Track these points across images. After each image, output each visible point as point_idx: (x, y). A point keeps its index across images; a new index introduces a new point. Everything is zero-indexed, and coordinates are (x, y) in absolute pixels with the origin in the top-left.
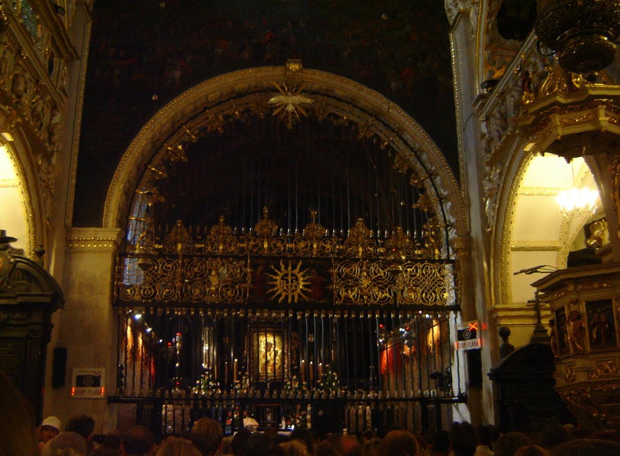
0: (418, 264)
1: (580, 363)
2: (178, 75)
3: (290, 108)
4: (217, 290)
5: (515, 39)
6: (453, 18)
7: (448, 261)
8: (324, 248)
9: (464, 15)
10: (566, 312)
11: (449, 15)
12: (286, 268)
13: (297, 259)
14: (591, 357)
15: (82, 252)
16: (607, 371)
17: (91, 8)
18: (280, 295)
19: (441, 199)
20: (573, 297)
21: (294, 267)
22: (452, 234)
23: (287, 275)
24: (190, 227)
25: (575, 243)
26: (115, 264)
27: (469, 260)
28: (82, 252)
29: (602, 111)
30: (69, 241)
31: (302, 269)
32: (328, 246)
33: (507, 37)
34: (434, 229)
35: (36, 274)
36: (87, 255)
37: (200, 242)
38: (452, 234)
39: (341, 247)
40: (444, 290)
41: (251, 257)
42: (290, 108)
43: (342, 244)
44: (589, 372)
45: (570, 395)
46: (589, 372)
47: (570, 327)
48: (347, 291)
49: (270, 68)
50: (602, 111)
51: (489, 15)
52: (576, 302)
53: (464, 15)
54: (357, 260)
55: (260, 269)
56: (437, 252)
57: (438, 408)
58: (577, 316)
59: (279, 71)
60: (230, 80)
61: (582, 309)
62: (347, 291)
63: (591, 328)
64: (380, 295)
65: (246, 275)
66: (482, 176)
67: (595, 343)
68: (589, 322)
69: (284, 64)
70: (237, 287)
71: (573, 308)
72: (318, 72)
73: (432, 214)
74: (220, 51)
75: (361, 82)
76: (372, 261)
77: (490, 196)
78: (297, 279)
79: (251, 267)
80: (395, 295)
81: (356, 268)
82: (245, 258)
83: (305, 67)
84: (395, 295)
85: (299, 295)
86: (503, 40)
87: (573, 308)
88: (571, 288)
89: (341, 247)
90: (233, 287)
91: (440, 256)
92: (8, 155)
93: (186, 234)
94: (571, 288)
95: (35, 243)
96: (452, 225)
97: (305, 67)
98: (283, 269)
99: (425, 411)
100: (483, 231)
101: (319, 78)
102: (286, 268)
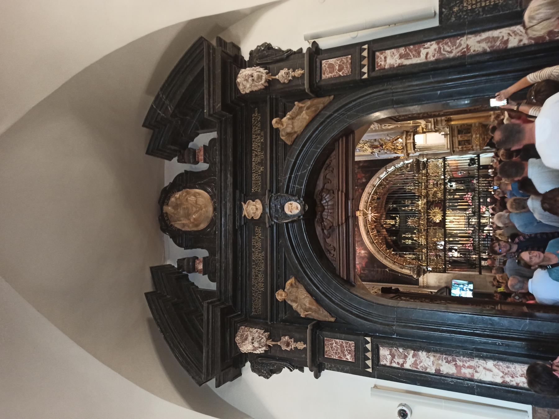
2: (363, 252)
15: (427, 282)
21: (430, 213)
28: (427, 282)
29: (408, 141)
30: (424, 287)
36: (429, 281)
42: (373, 214)
46: (476, 146)
52: (458, 148)
57: (482, 166)
58: (462, 148)
61: (460, 147)
63: (465, 145)
76: (427, 187)
81: (430, 192)
83: (358, 210)
97: (358, 210)
101: (362, 206)
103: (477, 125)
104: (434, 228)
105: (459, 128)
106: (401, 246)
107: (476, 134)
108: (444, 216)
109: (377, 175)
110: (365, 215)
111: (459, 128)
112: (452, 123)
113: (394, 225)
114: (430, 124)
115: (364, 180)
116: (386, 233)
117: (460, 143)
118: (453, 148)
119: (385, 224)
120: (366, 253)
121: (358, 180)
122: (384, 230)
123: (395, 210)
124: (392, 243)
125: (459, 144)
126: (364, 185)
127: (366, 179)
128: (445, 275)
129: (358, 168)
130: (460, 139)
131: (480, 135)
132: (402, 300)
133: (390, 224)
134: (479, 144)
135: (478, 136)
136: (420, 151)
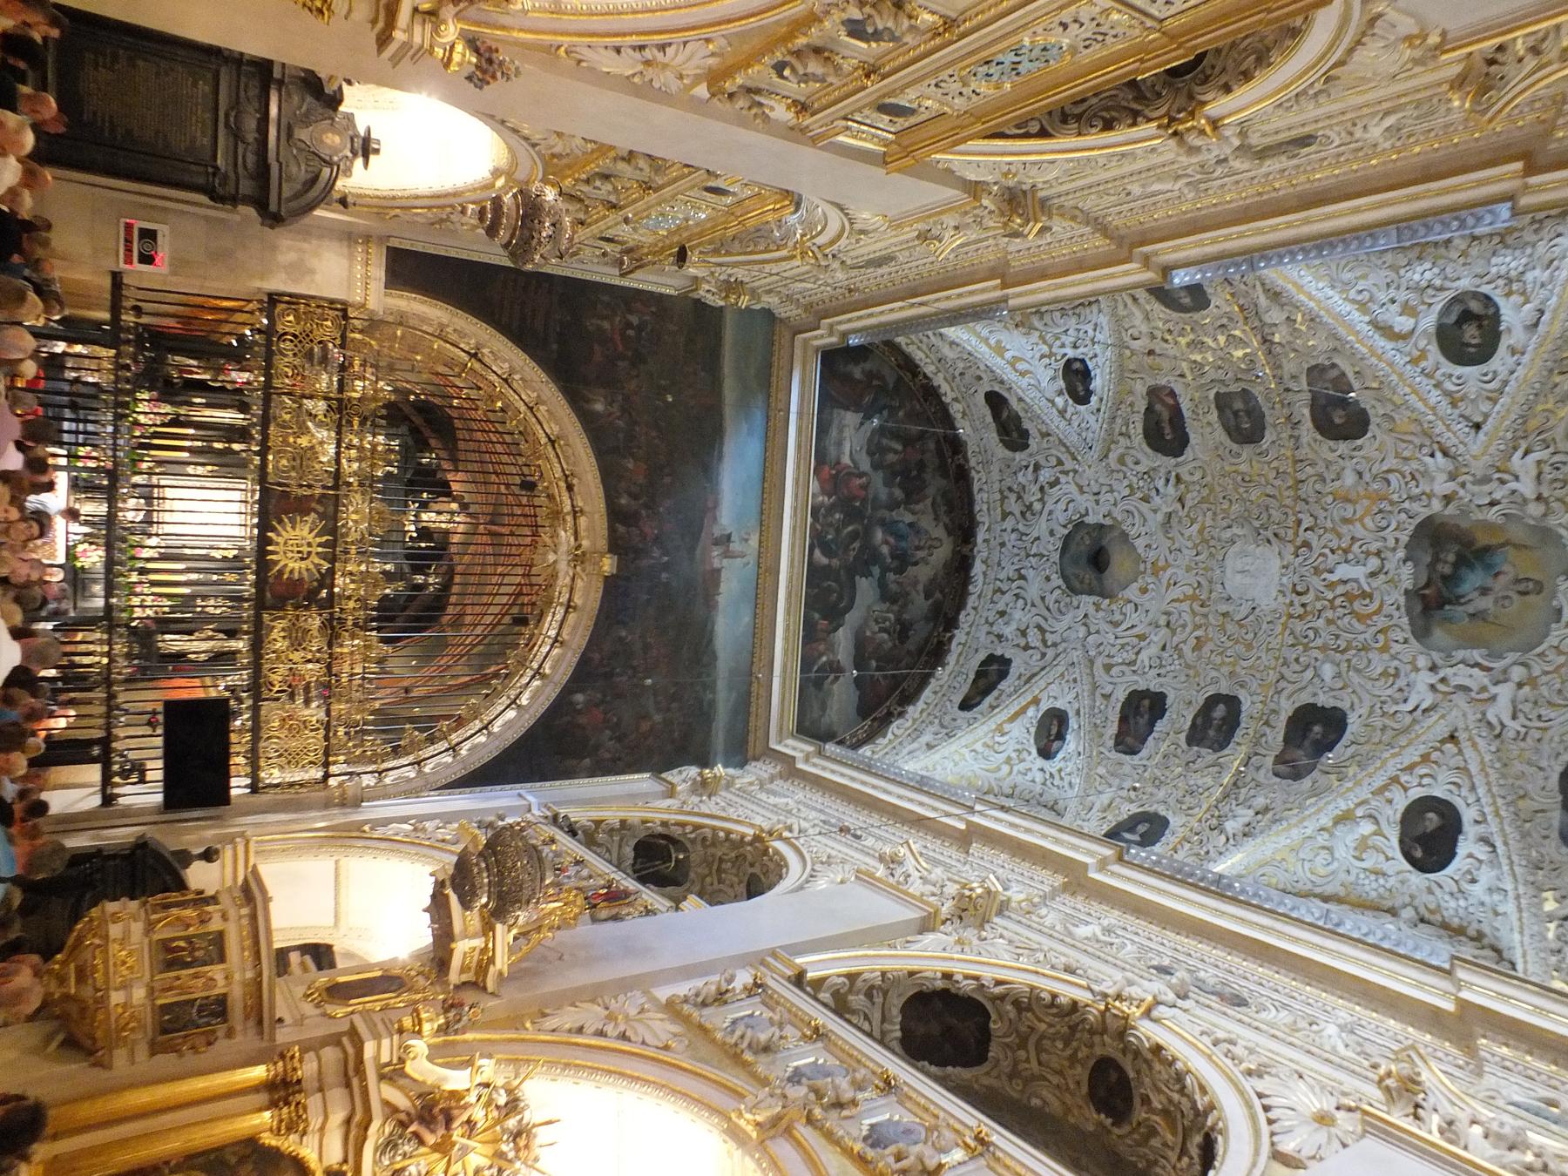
0: (322, 732)
1: (137, 928)
2: (599, 407)
3: (551, 557)
4: (289, 445)
5: (635, 858)
6: (670, 778)
7: (327, 776)
8: (349, 598)
9: (671, 793)
10: (210, 908)
11: (675, 771)
12: (320, 545)
13: (333, 559)
14: (146, 941)
16: (124, 963)
17: (695, 295)
18: (279, 535)
19: (418, 763)
20: (232, 913)
22: (368, 780)
23: (309, 544)
24: (384, 412)
25: (349, 955)
26: (332, 302)
27: (327, 805)
29: (478, 943)
31: (317, 566)
32: (351, 604)
33: (636, 849)
34: (375, 754)
35: (314, 193)
37: (362, 424)
38: (368, 780)
39: (350, 623)
40: (282, 767)
41: (337, 496)
43: (355, 625)
44: (124, 941)
45: (91, 920)
47: (189, 913)
48: (283, 630)
49: (606, 532)
50: (478, 943)
51: (664, 824)
52: (225, 917)
53: (671, 793)
54: (330, 646)
55: (320, 509)
56: (342, 758)
57: (93, 760)
59: (603, 543)
60: (590, 477)
61: (215, 925)
62: (283, 630)
63: (188, 939)
64: (275, 678)
65: (309, 486)
66: (447, 818)
67: (166, 946)
68: (194, 936)
69: (610, 551)
70: (293, 474)
71: (217, 918)
72: (600, 595)
73: (396, 752)
74: (631, 466)
75: (583, 654)
76: (329, 667)
77: (415, 830)
78: (302, 559)
79: (323, 495)
80: (277, 699)
82: (336, 487)
84: (277, 699)
85: (276, 563)
86: (633, 843)
87: (217, 918)
88: (245, 911)
89: (350, 623)
90: (294, 468)
91: (335, 763)
92: (479, 178)
93: (373, 406)
94: (245, 911)
95: (360, 196)
96: (380, 780)
98: (318, 540)
99: (90, 743)
100: (366, 822)
101: (588, 596)
102: (320, 545)
103: (120, 1057)
104: (309, 492)
105: (221, 1030)
106: (404, 429)
107: (125, 1006)
108: (263, 542)
109: (528, 721)
110: (578, 558)
111: (221, 1030)
112: (259, 1072)
113: (424, 506)
114: (385, 1058)
115: (579, 697)
116: (450, 477)
117: (217, 948)
118: (253, 917)
119: (452, 513)
120: (588, 401)
121: (602, 702)
122: (455, 487)
123: (419, 561)
124: (433, 442)
125: (220, 937)
126: (583, 674)
127: (571, 703)
128: (278, 283)
129: (597, 747)
130: (216, 972)
131: (102, 1002)
132: (496, 173)
133: (439, 513)
134: (114, 948)
135: (116, 998)
136: (359, 826)
